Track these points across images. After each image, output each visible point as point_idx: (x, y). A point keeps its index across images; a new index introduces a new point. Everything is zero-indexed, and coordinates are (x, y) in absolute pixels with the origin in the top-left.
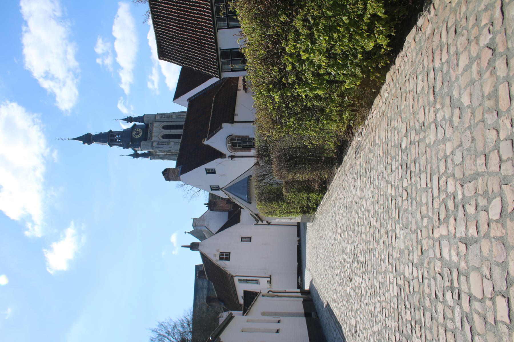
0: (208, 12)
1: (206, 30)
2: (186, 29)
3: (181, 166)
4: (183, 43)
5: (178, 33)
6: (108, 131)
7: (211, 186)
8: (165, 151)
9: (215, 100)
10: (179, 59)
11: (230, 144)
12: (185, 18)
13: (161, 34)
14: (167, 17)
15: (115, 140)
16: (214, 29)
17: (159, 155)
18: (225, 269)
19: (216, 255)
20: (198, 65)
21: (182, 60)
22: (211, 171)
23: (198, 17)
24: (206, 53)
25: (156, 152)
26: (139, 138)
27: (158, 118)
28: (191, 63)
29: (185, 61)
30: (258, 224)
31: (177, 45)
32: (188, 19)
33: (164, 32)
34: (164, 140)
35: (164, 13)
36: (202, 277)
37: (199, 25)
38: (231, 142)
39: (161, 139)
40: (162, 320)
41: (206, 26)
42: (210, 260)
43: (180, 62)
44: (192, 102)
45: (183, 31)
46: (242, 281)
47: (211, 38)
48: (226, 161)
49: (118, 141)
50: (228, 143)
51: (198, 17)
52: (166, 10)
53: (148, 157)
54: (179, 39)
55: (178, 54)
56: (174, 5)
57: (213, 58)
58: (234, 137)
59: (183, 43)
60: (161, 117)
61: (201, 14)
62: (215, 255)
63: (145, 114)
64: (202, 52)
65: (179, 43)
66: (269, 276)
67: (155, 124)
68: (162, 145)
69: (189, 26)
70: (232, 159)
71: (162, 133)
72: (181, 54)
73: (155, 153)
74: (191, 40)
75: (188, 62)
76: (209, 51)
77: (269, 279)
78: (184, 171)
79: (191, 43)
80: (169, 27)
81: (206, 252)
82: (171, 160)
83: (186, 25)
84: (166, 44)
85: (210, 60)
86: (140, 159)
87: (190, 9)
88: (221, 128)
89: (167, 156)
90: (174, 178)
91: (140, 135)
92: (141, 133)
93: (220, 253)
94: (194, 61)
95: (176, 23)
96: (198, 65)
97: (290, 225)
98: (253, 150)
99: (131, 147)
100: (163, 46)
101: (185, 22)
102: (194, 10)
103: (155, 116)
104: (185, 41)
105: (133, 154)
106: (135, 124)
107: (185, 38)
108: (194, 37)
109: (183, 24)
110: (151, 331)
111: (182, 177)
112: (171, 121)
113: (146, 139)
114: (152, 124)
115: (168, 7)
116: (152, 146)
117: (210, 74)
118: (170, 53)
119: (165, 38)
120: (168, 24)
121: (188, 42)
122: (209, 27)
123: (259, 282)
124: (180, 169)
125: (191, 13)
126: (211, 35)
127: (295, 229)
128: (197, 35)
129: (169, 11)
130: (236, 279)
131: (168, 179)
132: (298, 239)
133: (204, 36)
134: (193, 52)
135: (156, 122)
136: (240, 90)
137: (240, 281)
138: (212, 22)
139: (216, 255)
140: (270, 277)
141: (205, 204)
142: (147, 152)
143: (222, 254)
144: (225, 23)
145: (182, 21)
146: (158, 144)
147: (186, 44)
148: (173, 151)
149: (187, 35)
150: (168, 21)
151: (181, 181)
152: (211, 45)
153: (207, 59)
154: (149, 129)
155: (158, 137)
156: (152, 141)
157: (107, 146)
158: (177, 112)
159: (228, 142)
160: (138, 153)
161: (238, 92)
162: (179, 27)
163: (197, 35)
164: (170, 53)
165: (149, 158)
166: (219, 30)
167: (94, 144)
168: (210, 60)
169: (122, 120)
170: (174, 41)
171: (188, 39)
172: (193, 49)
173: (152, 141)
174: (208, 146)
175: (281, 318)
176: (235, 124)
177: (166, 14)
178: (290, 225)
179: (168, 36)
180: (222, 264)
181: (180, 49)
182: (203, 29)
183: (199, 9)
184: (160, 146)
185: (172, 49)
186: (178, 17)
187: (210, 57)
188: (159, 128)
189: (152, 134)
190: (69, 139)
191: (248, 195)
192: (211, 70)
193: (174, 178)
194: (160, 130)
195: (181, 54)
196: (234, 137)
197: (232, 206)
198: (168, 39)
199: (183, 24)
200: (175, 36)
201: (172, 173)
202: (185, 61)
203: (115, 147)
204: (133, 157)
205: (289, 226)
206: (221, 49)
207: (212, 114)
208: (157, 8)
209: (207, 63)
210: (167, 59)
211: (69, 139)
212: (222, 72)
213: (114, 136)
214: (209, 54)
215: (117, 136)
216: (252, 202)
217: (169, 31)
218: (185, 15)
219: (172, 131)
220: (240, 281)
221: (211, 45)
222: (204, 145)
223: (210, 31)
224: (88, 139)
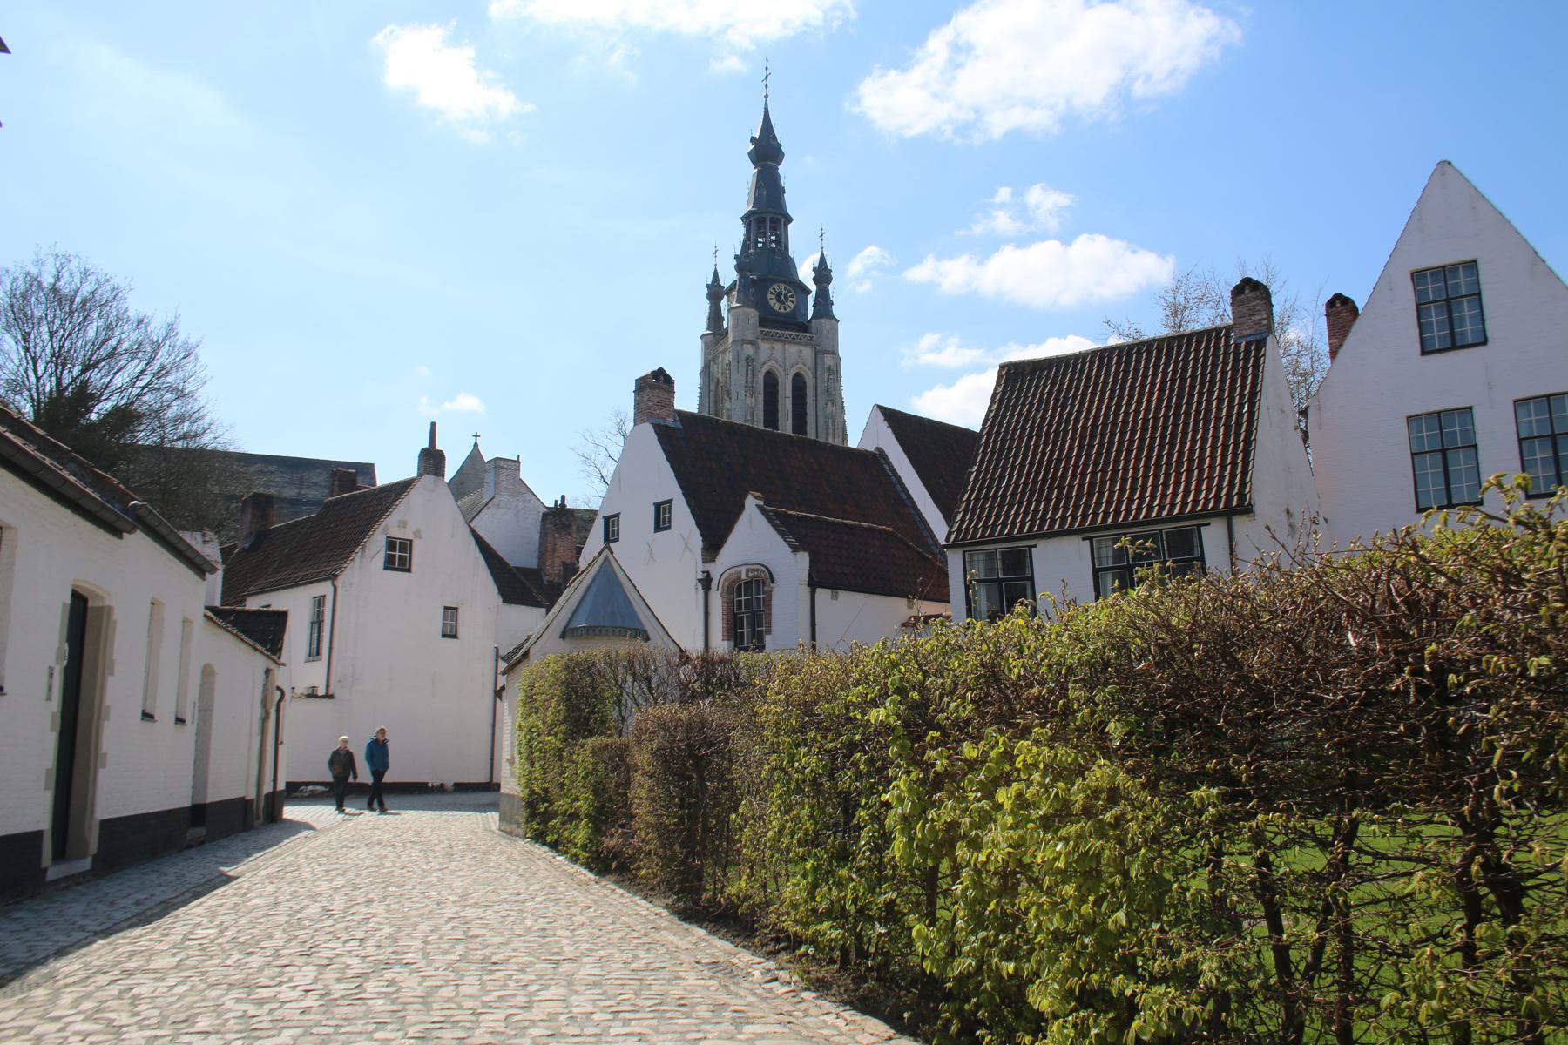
0: (1139, 509)
1: (1087, 505)
2: (1091, 446)
3: (679, 425)
4: (1048, 435)
5: (1077, 421)
6: (790, 210)
7: (617, 515)
8: (728, 381)
9: (880, 530)
10: (1001, 425)
11: (747, 576)
12: (1121, 442)
13: (1073, 372)
14: (1122, 389)
16: (1092, 529)
17: (714, 360)
18: (358, 556)
19: (404, 527)
20: (984, 480)
21: (998, 433)
22: (664, 518)
23: (1124, 480)
24: (1020, 504)
25: (723, 352)
27: (828, 361)
28: (990, 461)
29: (995, 442)
30: (497, 661)
31: (1043, 418)
32: (1119, 452)
33: (1079, 380)
34: (761, 377)
35: (1134, 379)
36: (336, 483)
37: (1103, 482)
38: (752, 578)
40: (204, 354)
41: (1098, 504)
42: (388, 508)
43: (992, 426)
44: (874, 461)
45: (1082, 437)
46: (319, 606)
47: (1064, 518)
48: (693, 563)
50: (747, 571)
51: (1124, 480)
52: (1143, 386)
53: (708, 329)
54: (1059, 423)
55: (1017, 422)
56: (1158, 409)
57: (1004, 524)
58: (766, 588)
59: (1048, 435)
60: (829, 369)
61: (1133, 490)
62: (403, 524)
64: (1023, 493)
65: (1050, 425)
66: (330, 693)
67: (808, 352)
69: (1099, 454)
70: (699, 580)
71: (781, 370)
72: (1015, 431)
74: (1059, 460)
75: (993, 452)
76: (1026, 513)
77: (321, 692)
78: (664, 434)
79: (1050, 461)
80: (1093, 394)
81: (414, 495)
82: (701, 397)
83: (1101, 444)
84: (1045, 386)
85: (998, 516)
86: (706, 305)
87: (1149, 458)
88: (795, 549)
89: (712, 388)
90: (642, 405)
91: (777, 305)
92: (782, 310)
93: (411, 541)
94: (995, 469)
95: (1106, 415)
96: (984, 480)
97: (492, 760)
98: (729, 647)
99: (740, 278)
100: (1040, 378)
101: (1111, 443)
102: (1147, 467)
103: (834, 353)
104: (1055, 443)
105: (719, 284)
106: (808, 292)
107: (1064, 442)
108: (1066, 469)
109: (1103, 435)
110: (169, 321)
111: (648, 429)
113: (763, 322)
114: (809, 342)
115: (1151, 393)
116: (744, 342)
117: (959, 518)
118: (1018, 398)
119: (1062, 384)
120: (1103, 393)
121: (1052, 452)
122: (1095, 514)
124: (670, 422)
125: (1138, 459)
126: (1074, 518)
127: (481, 777)
128: (1073, 476)
129: (1141, 395)
130: (324, 588)
131: (642, 385)
132: (449, 784)
133: (1069, 498)
134: (1022, 465)
136: (911, 607)
138: (1113, 521)
139: (404, 527)
140: (329, 696)
141: (563, 498)
142: (725, 325)
143: (406, 545)
144: (1111, 560)
145: (1113, 435)
147: (1046, 445)
148: (727, 405)
149: (1071, 448)
150: (1112, 391)
152: (1043, 520)
153: (1001, 506)
156: (759, 341)
157: (744, 205)
158: (846, 417)
159: (753, 570)
161: (904, 601)
162: (1094, 425)
163: (1073, 476)
164: (1018, 398)
166: (1088, 542)
167: (751, 171)
168: (998, 516)
170: (1055, 409)
171: (1061, 450)
172: (1031, 464)
173: (759, 341)
174: (742, 508)
175: (190, 729)
176: (805, 592)
177: (1132, 387)
178: (492, 760)
179: (1069, 390)
180: (376, 544)
181: (1032, 427)
182: (1090, 495)
183: (1150, 483)
184: (743, 363)
185: (1031, 404)
186: (1125, 422)
187: (1007, 515)
189: (779, 341)
190: (766, 97)
191: (588, 629)
192: (971, 521)
193: (642, 405)
194: (792, 367)
195: (1015, 431)
196: (766, 588)
197: (557, 580)
198: (1059, 391)
199: (1103, 435)
200: (1070, 414)
201: (658, 399)
202: (995, 442)
203: (740, 231)
204: (710, 282)
205: (489, 758)
206: (1033, 549)
207: (838, 523)
208: (1148, 360)
209: (992, 507)
210: (1000, 389)
211: (766, 97)
212: (964, 552)
213: (774, 229)
214: (1017, 514)
215: (773, 238)
216: (567, 640)
217: (1084, 395)
218: (1131, 441)
220: (320, 601)
221: (1043, 520)
222: (745, 497)
223: (1085, 516)
224: (766, 152)
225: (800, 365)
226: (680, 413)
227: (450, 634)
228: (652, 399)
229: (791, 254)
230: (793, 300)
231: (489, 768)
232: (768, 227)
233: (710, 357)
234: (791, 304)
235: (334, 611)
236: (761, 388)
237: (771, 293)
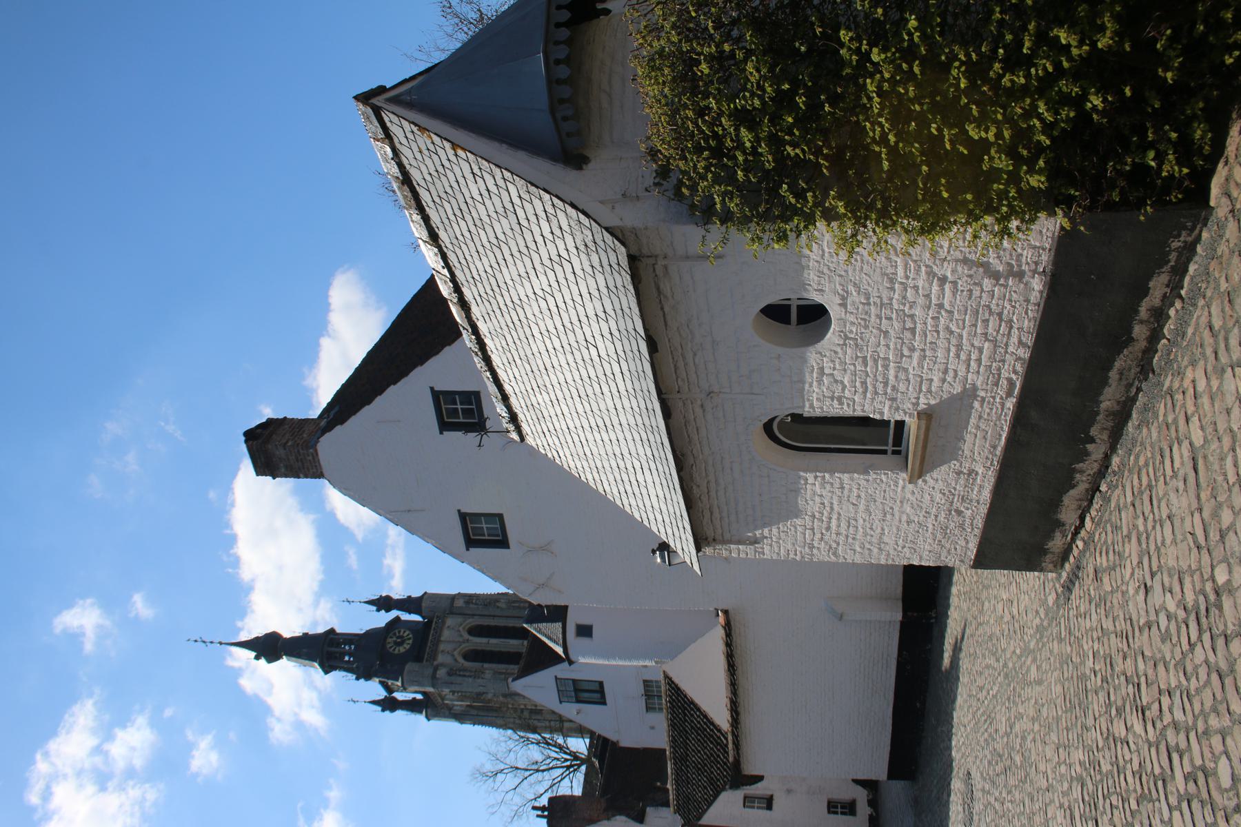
7: (464, 517)
8: (468, 694)
15: (338, 655)
17: (450, 708)
25: (443, 699)
26: (403, 653)
27: (459, 603)
34: (467, 664)
39: (461, 660)
49: (347, 658)
53: (421, 712)
60: (467, 603)
63: (426, 593)
67: (450, 621)
68: (460, 675)
71: (464, 645)
73: (440, 700)
86: (400, 714)
91: (405, 645)
92: (411, 641)
99: (377, 677)
103: (453, 598)
105: (382, 700)
106: (397, 619)
112: (492, 614)
116: (434, 677)
135: (452, 613)
141: (534, 808)
142: (419, 697)
146: (449, 674)
148: (490, 696)
151: (319, 475)
154: (432, 632)
155: (453, 656)
156: (435, 663)
160: (395, 699)
165: (424, 712)
167: (284, 662)
173: (435, 663)
184: (453, 679)
188: (459, 631)
190: (221, 643)
194: (461, 636)
203: (337, 675)
204: (380, 708)
211: (221, 643)
213: (338, 645)
219: (493, 641)
225: (461, 629)
226: (321, 416)
228: (284, 441)
229: (362, 632)
230: (402, 631)
232: (337, 650)
233: (447, 713)
234: (405, 634)
236: (477, 665)
237: (394, 650)
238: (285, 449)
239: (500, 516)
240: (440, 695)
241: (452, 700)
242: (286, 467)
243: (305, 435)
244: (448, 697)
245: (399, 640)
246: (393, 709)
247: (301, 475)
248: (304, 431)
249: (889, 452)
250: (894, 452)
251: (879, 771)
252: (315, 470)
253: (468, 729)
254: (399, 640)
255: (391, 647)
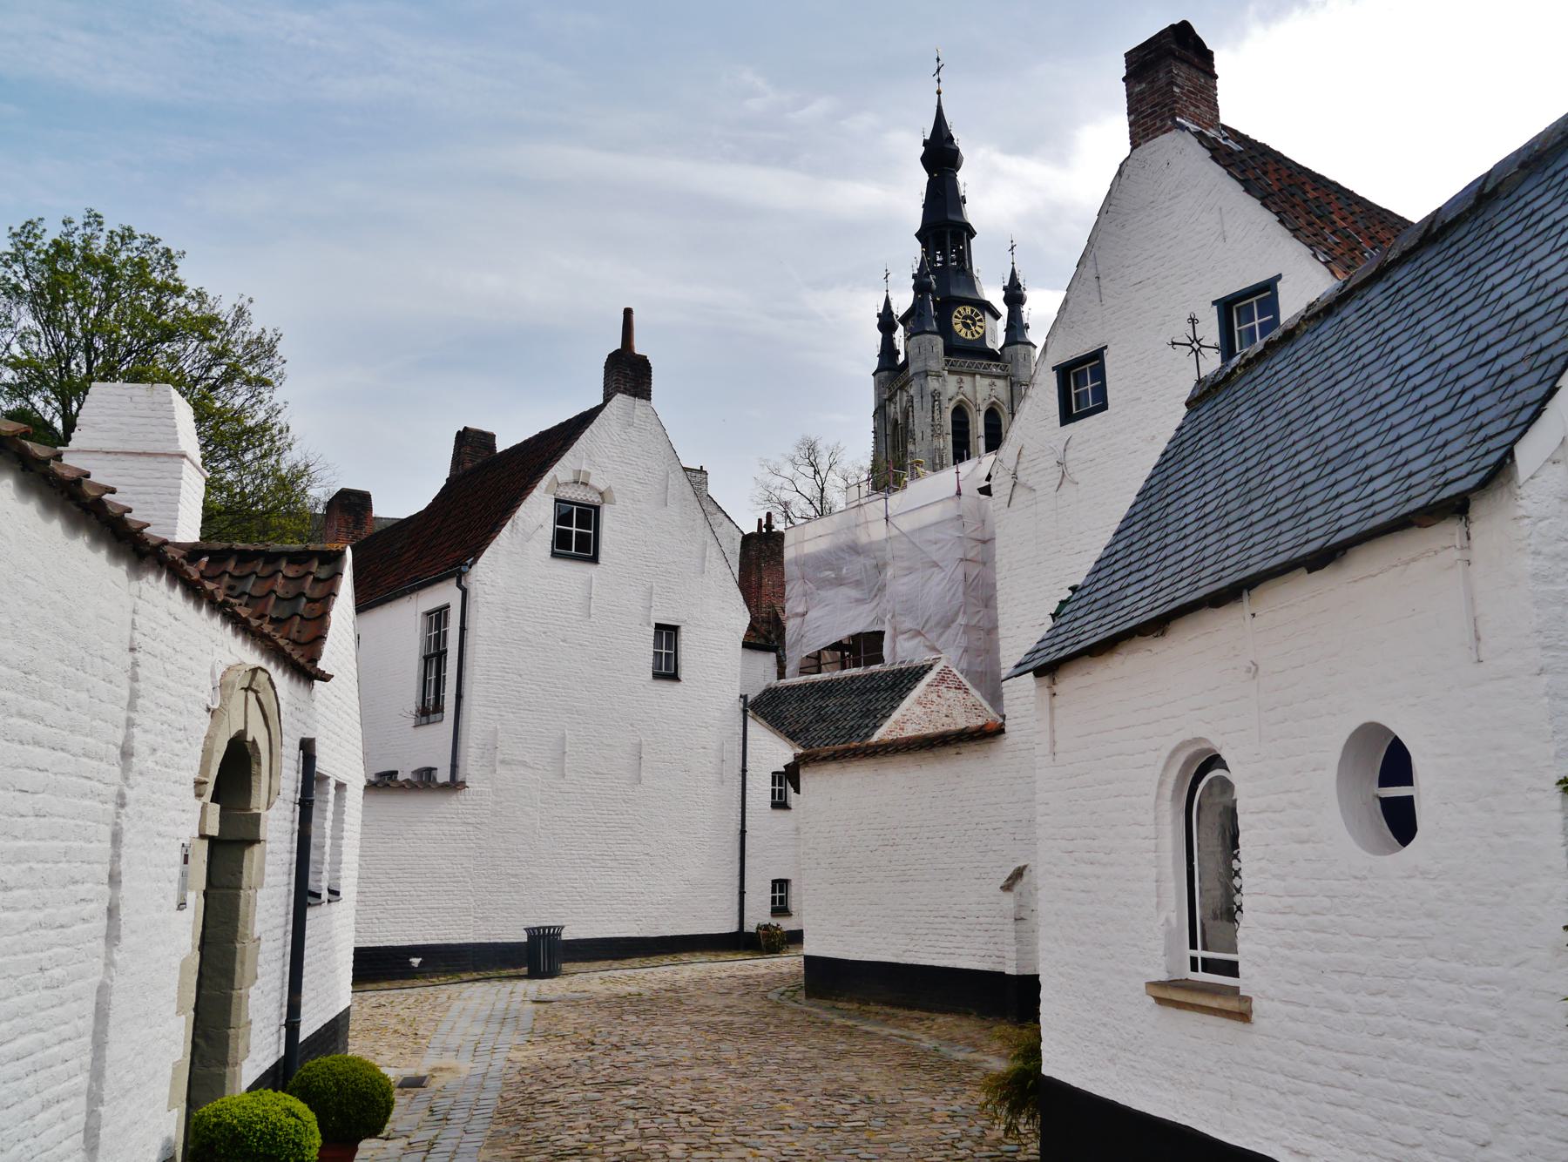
7: (1097, 356)
8: (911, 420)
17: (890, 399)
34: (948, 416)
39: (952, 405)
46: (438, 627)
67: (1000, 384)
68: (933, 407)
77: (443, 776)
91: (964, 330)
92: (970, 337)
93: (597, 509)
97: (742, 893)
106: (997, 316)
113: (949, 351)
123: (428, 723)
127: (725, 924)
130: (445, 594)
135: (1012, 385)
137: (438, 618)
141: (769, 516)
142: (901, 358)
148: (911, 447)
151: (1135, 145)
160: (895, 328)
167: (924, 177)
169: (1013, 270)
190: (939, 93)
203: (916, 249)
204: (881, 311)
211: (939, 93)
220: (438, 617)
226: (1225, 128)
227: (667, 670)
229: (975, 272)
231: (736, 907)
233: (886, 396)
234: (978, 328)
235: (463, 629)
237: (956, 317)
238: (1168, 84)
239: (1104, 407)
240: (907, 382)
241: (901, 400)
242: (1142, 92)
243: (1192, 108)
244: (905, 394)
245: (969, 321)
246: (881, 327)
247: (1132, 117)
248: (1198, 107)
249: (1193, 953)
250: (1194, 960)
251: (811, 947)
252: (1141, 135)
253: (869, 425)
254: (969, 321)
255: (959, 312)
